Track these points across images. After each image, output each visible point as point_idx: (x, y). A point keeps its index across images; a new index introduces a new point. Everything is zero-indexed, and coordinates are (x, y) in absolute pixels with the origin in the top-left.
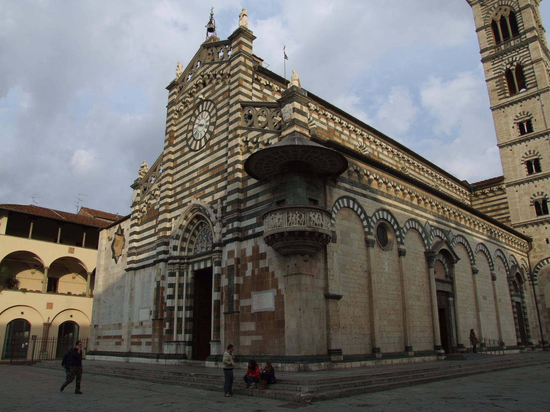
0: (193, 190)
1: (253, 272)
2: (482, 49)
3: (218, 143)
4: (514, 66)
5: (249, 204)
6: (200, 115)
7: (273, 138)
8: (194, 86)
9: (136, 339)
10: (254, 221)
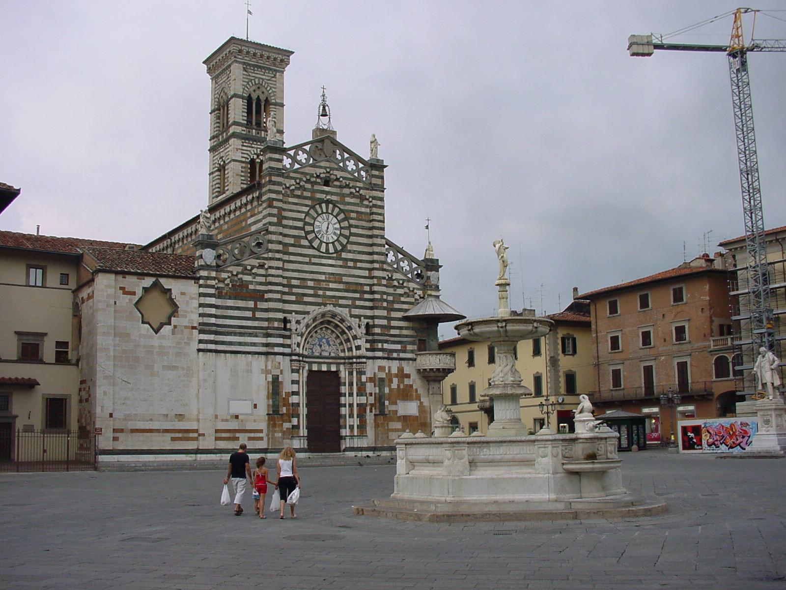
0: (320, 292)
1: (399, 386)
2: (236, 120)
3: (355, 261)
4: (260, 159)
5: (393, 332)
6: (324, 215)
7: (418, 289)
8: (315, 175)
9: (232, 434)
10: (398, 347)
